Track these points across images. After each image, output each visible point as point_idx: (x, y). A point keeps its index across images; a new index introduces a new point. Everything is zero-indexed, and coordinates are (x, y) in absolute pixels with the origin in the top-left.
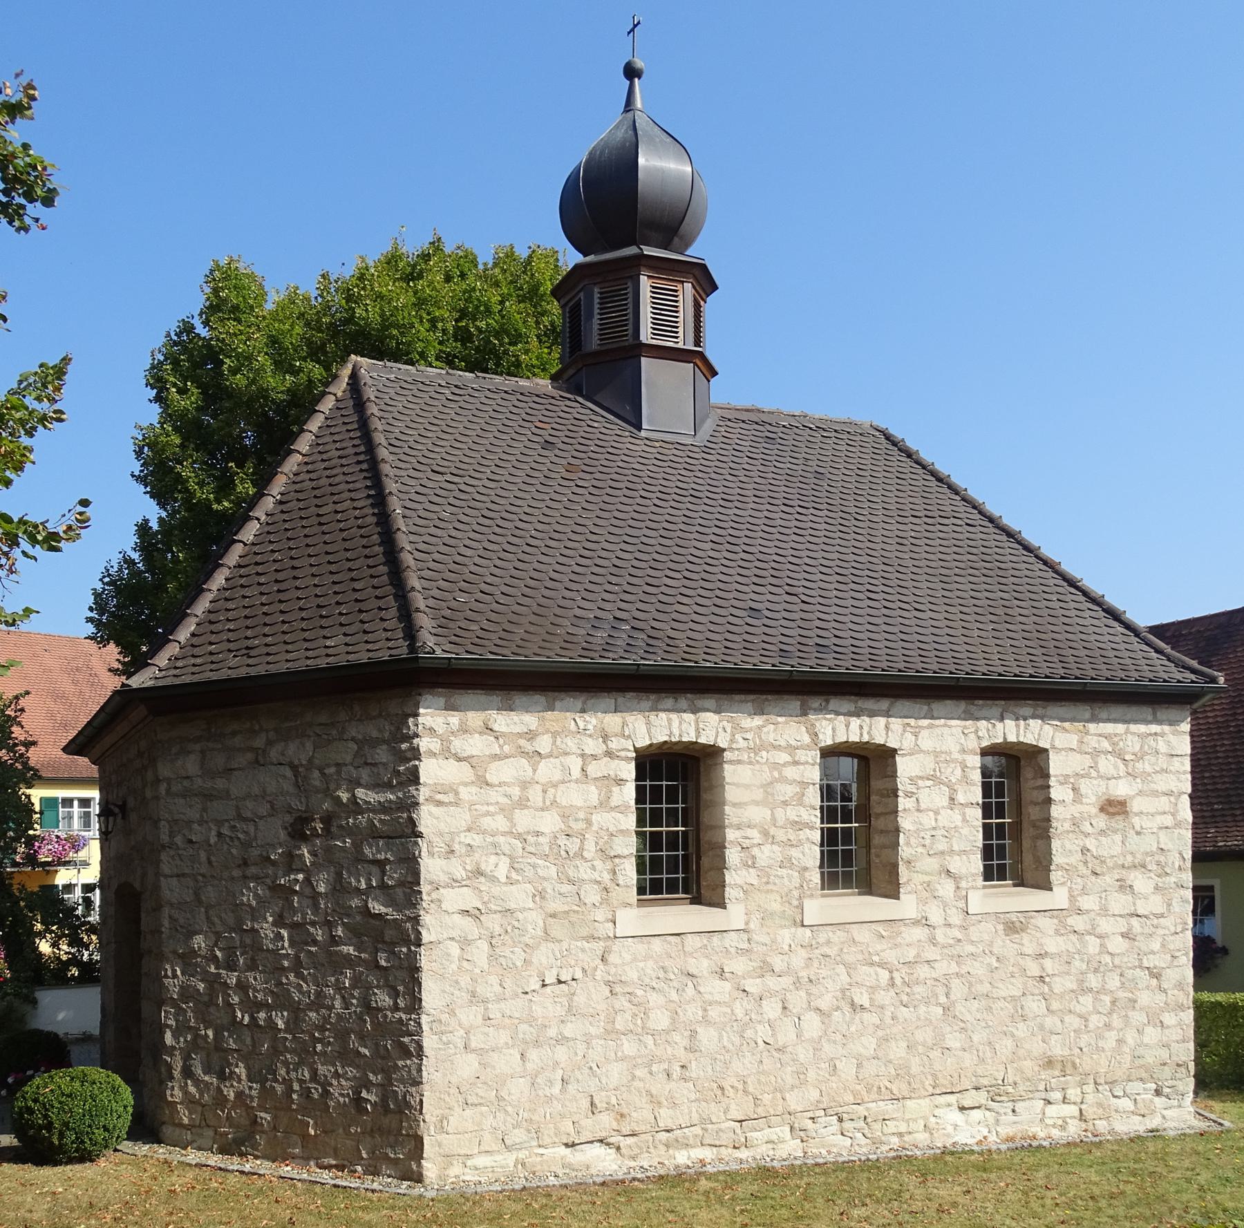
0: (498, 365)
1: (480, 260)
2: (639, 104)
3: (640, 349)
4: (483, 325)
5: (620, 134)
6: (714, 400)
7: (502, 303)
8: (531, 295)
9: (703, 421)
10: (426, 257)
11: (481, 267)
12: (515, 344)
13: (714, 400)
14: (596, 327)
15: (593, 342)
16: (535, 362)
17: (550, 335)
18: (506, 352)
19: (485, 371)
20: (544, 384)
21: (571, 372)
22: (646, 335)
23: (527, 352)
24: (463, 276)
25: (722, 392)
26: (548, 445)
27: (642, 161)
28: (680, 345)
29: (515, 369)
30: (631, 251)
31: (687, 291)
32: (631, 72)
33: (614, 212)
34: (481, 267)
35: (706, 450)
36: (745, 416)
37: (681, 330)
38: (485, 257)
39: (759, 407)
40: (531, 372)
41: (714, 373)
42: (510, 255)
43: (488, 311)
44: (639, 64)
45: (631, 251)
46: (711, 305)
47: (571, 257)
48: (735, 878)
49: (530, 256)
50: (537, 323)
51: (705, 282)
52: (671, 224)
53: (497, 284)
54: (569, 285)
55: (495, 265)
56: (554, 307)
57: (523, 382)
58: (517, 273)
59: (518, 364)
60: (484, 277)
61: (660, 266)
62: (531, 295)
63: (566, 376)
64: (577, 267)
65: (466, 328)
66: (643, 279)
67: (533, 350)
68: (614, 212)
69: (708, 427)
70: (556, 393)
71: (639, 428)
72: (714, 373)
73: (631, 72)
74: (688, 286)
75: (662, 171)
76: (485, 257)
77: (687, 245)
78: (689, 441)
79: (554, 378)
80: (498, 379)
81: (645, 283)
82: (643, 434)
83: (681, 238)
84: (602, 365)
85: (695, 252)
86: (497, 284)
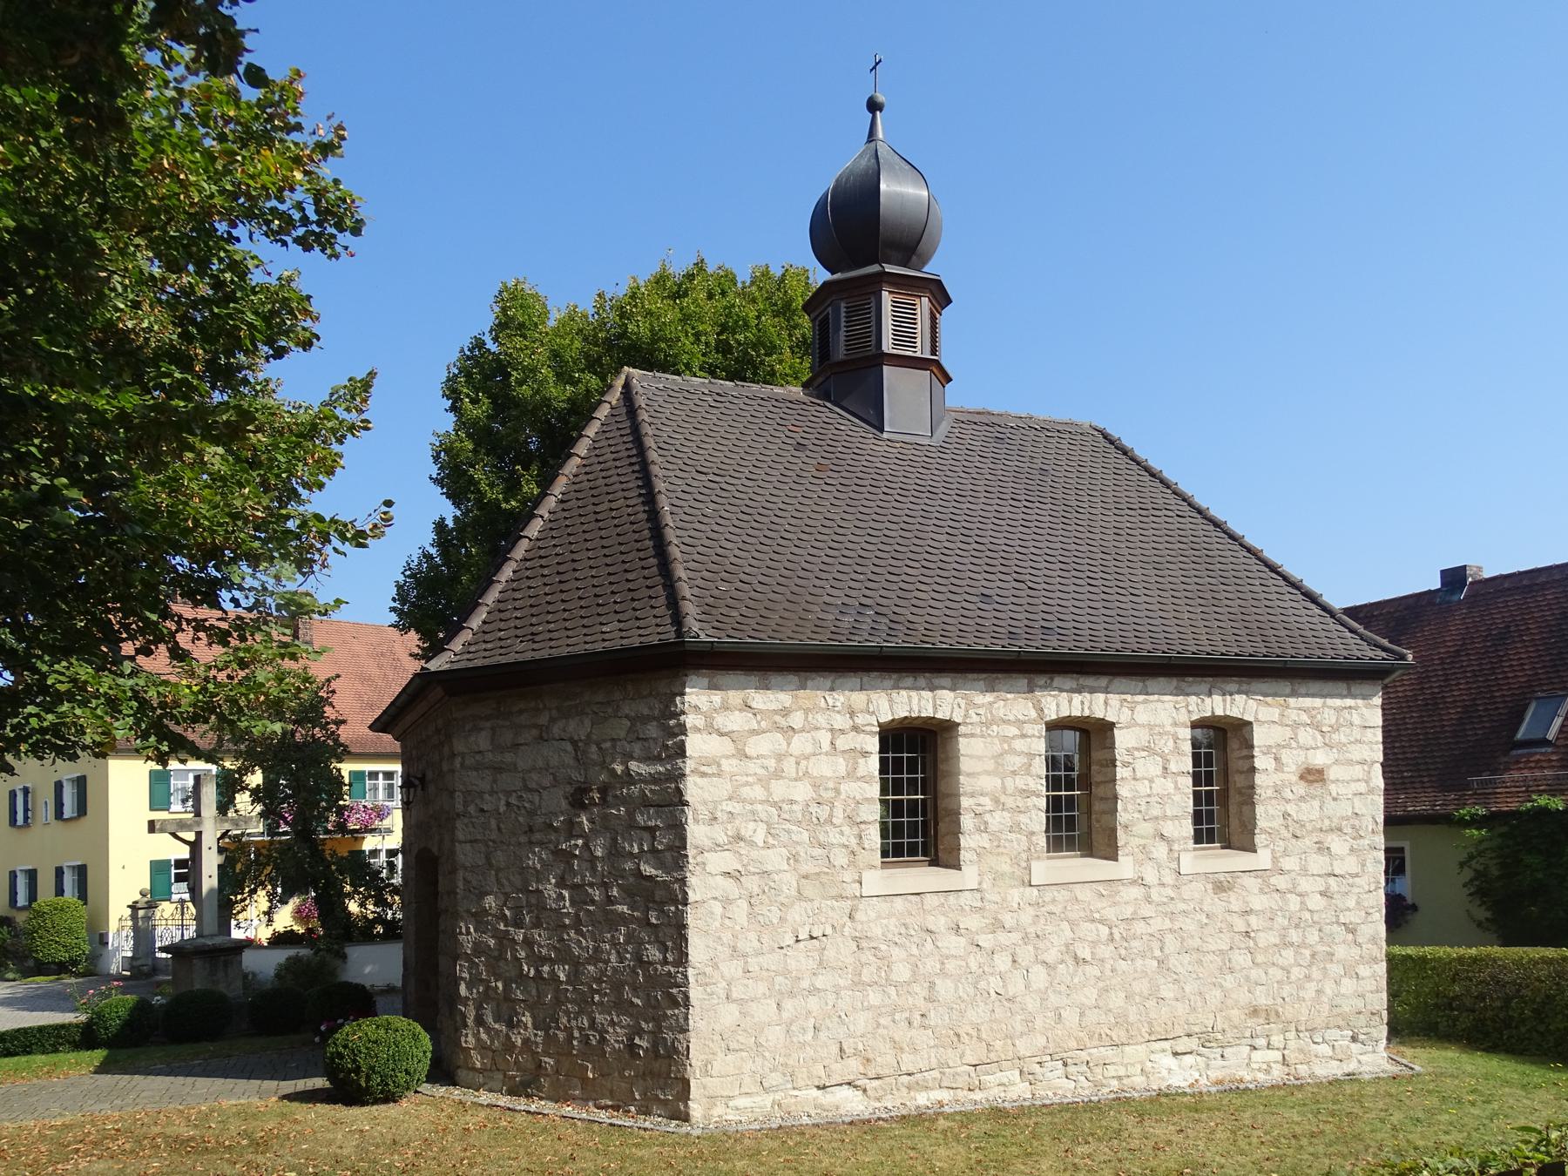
0: (755, 374)
1: (739, 279)
2: (880, 135)
3: (881, 359)
4: (741, 337)
5: (864, 162)
6: (951, 402)
7: (758, 317)
8: (784, 311)
9: (939, 423)
10: (690, 277)
11: (739, 285)
12: (769, 355)
13: (951, 402)
14: (842, 338)
15: (840, 352)
16: (788, 371)
17: (802, 347)
18: (762, 362)
19: (744, 379)
20: (796, 391)
21: (820, 380)
22: (888, 346)
23: (781, 362)
24: (723, 293)
25: (957, 396)
26: (800, 446)
27: (883, 186)
28: (918, 354)
29: (770, 378)
30: (874, 268)
31: (924, 304)
32: (874, 106)
33: (862, 237)
34: (739, 285)
35: (942, 449)
36: (977, 419)
37: (919, 340)
38: (743, 276)
39: (990, 409)
40: (785, 379)
41: (949, 380)
42: (766, 274)
43: (746, 325)
44: (881, 98)
45: (875, 268)
46: (947, 317)
47: (820, 275)
48: (969, 841)
50: (790, 335)
51: (941, 297)
52: (910, 244)
53: (754, 301)
54: (820, 300)
55: (753, 283)
56: (805, 321)
57: (777, 390)
58: (772, 289)
59: (773, 373)
60: (742, 294)
61: (900, 282)
62: (784, 311)
63: (816, 384)
64: (825, 284)
65: (727, 341)
66: (885, 294)
67: (786, 360)
68: (862, 237)
69: (943, 429)
70: (807, 399)
71: (882, 431)
72: (949, 380)
73: (874, 106)
74: (925, 300)
75: (902, 195)
76: (743, 276)
77: (924, 263)
78: (926, 442)
79: (805, 386)
80: (755, 387)
81: (887, 298)
82: (885, 435)
83: (919, 256)
84: (848, 373)
85: (932, 269)
86: (754, 301)
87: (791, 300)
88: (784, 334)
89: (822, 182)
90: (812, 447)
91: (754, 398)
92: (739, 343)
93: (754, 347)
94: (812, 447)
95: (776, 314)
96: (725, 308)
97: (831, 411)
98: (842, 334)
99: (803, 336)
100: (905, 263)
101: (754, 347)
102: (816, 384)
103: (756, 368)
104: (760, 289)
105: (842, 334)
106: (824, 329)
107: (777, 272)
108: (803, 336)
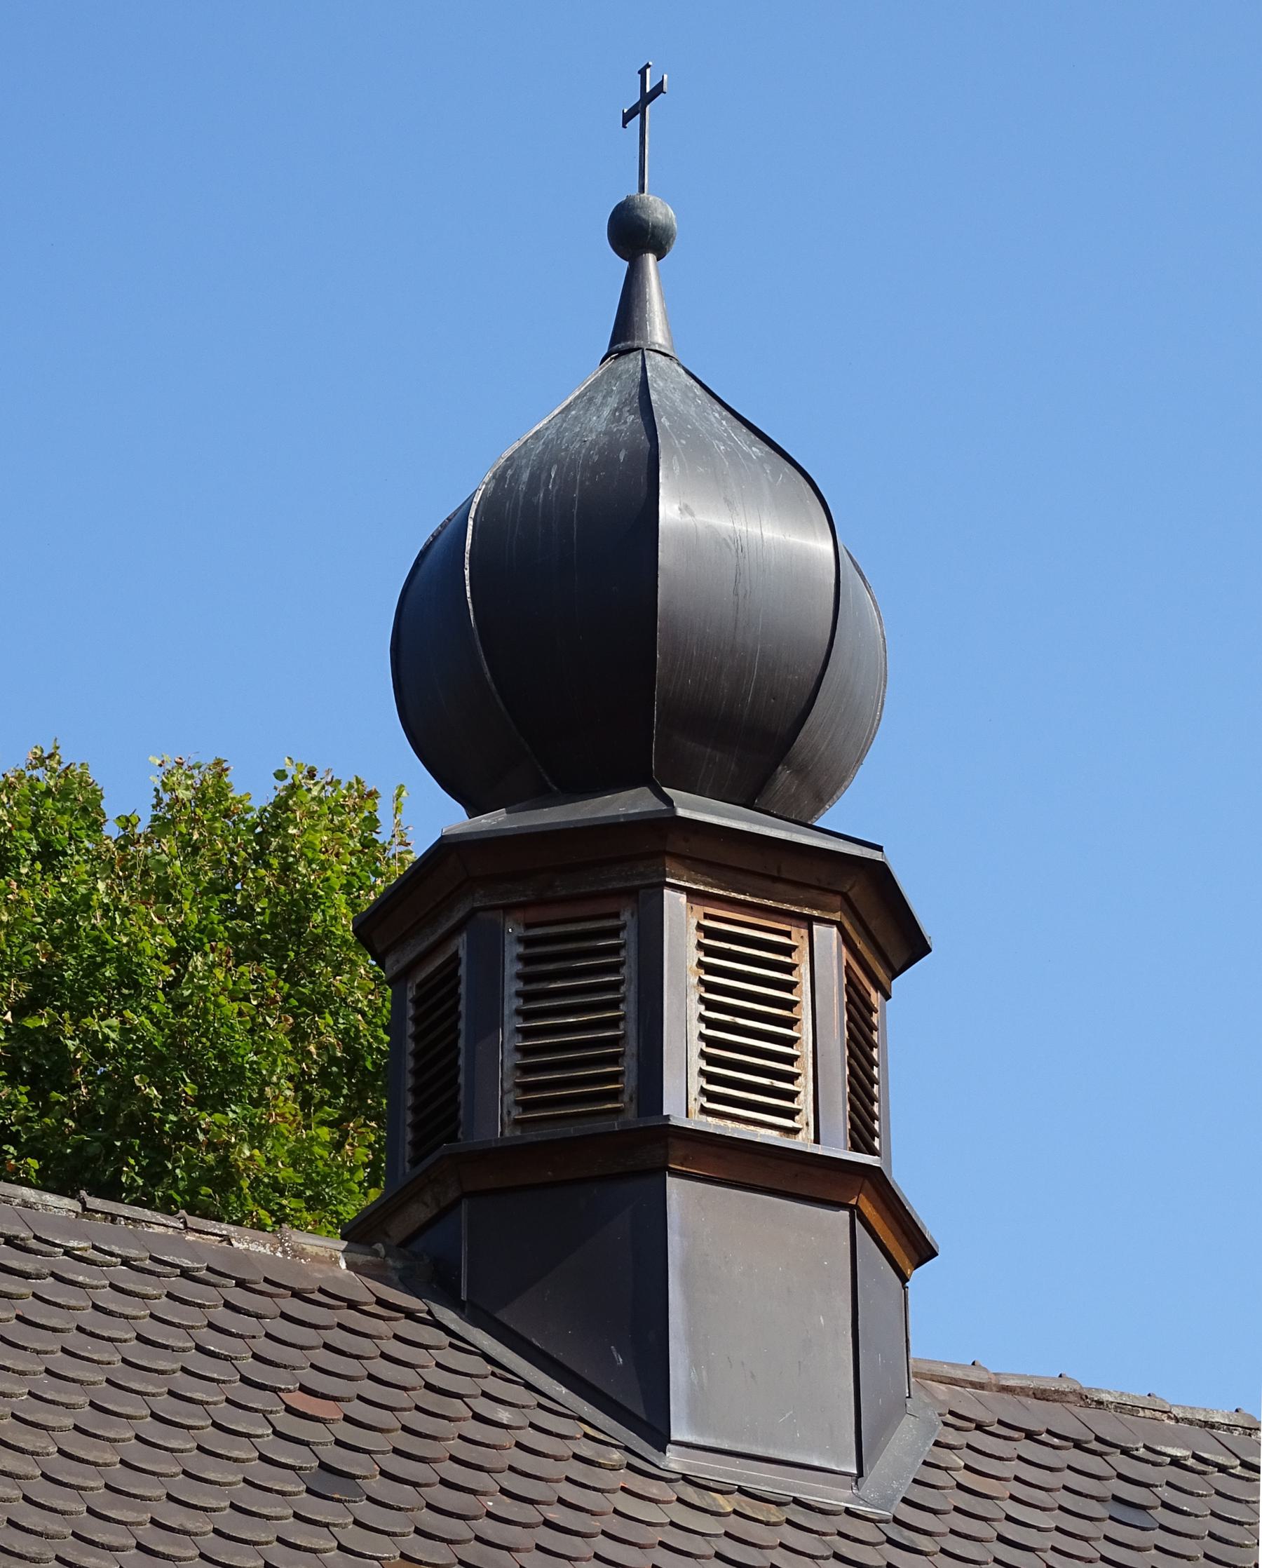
0: (155, 1175)
1: (112, 808)
2: (657, 331)
3: (659, 1151)
4: (109, 1029)
5: (598, 422)
6: (928, 1346)
7: (178, 956)
8: (282, 938)
9: (888, 1423)
11: (112, 830)
12: (219, 1104)
13: (928, 1346)
14: (508, 1060)
15: (500, 1107)
16: (285, 1173)
17: (342, 1080)
18: (186, 1131)
19: (111, 1191)
20: (321, 1253)
21: (419, 1213)
22: (683, 1098)
23: (258, 1135)
24: (49, 856)
25: (957, 1319)
26: (331, 1480)
27: (669, 511)
28: (803, 1142)
29: (216, 1192)
30: (632, 803)
31: (823, 953)
32: (634, 235)
33: (572, 665)
34: (112, 830)
35: (900, 1535)
36: (1035, 1416)
37: (804, 1086)
38: (128, 798)
39: (1086, 1380)
40: (272, 1206)
41: (923, 1251)
42: (213, 796)
43: (130, 979)
44: (660, 209)
45: (632, 803)
46: (907, 1004)
47: (423, 815)
49: (281, 805)
50: (297, 1034)
51: (888, 932)
52: (769, 720)
53: (164, 893)
54: (420, 907)
55: (161, 826)
56: (360, 985)
57: (247, 1243)
58: (238, 864)
59: (224, 1177)
60: (121, 864)
61: (738, 867)
62: (282, 938)
63: (399, 1229)
64: (446, 848)
65: (51, 1039)
66: (674, 902)
67: (279, 1129)
68: (572, 665)
69: (904, 1448)
70: (362, 1288)
72: (923, 1251)
73: (634, 235)
74: (827, 936)
75: (737, 547)
76: (128, 798)
77: (823, 797)
78: (837, 1496)
79: (358, 1234)
80: (160, 1225)
81: (681, 920)
82: (674, 1460)
83: (801, 771)
84: (528, 1199)
85: (854, 816)
86: (164, 893)
87: (305, 902)
88: (277, 1027)
89: (445, 481)
90: (378, 1486)
91: (157, 1267)
92: (98, 1049)
93: (158, 1066)
94: (378, 1486)
95: (247, 950)
96: (54, 911)
97: (459, 1343)
98: (508, 1038)
99: (349, 1038)
100: (750, 796)
101: (158, 1066)
102: (399, 1229)
103: (158, 1152)
104: (191, 849)
105: (508, 1038)
106: (436, 1023)
107: (254, 791)
108: (349, 1038)
